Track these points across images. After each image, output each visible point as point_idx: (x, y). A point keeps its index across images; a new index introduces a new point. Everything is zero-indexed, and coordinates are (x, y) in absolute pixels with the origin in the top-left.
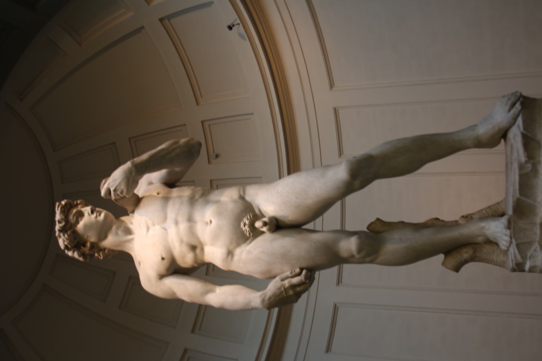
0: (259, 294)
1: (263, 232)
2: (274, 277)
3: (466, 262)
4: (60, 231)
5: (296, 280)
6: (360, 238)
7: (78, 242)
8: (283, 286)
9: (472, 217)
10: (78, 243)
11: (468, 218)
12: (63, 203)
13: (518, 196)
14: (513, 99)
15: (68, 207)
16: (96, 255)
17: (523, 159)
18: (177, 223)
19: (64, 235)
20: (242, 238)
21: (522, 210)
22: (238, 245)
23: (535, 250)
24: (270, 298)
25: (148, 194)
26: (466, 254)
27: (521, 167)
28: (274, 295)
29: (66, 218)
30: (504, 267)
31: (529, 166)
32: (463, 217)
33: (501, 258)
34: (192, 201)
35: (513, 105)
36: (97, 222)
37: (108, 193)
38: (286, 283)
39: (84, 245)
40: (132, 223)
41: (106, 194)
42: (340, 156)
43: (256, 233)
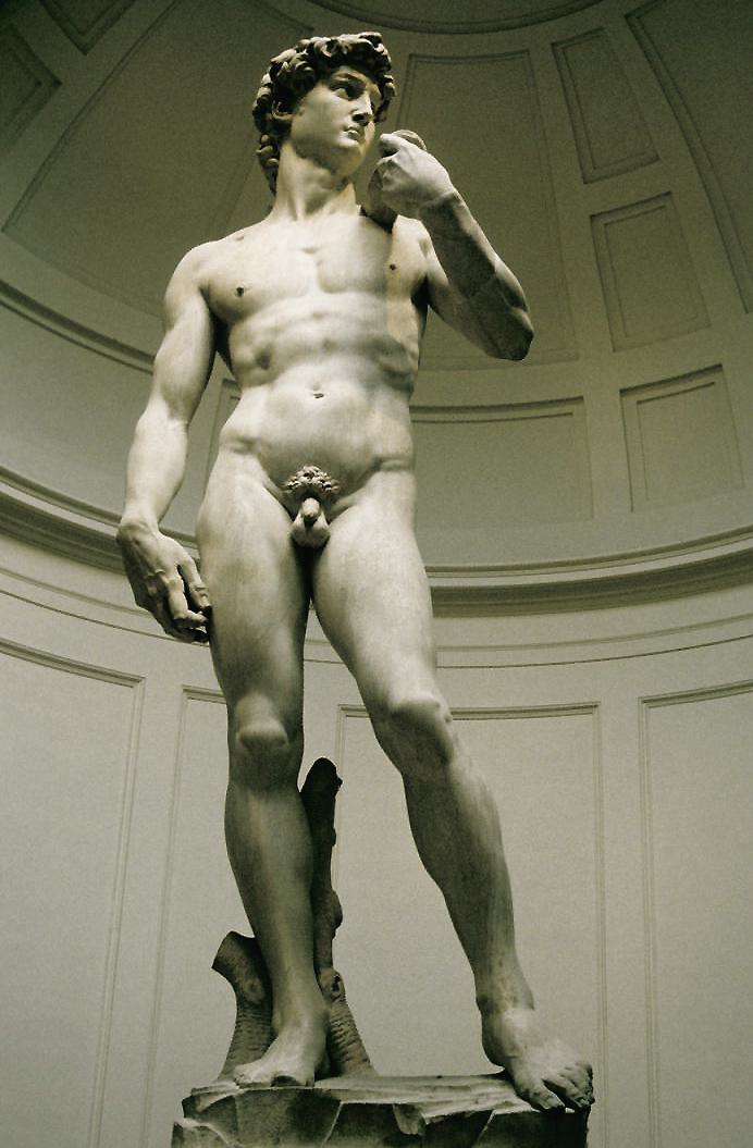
0: (151, 518)
1: (293, 517)
3: (236, 987)
5: (179, 600)
6: (281, 742)
7: (290, 90)
8: (166, 571)
9: (334, 999)
12: (380, 48)
13: (342, 1103)
16: (265, 138)
17: (428, 1115)
18: (318, 316)
19: (303, 58)
20: (279, 469)
24: (138, 543)
25: (396, 245)
27: (409, 1110)
28: (146, 551)
29: (343, 57)
30: (223, 1072)
31: (415, 1129)
32: (338, 979)
34: (375, 349)
36: (335, 132)
37: (389, 149)
38: (174, 578)
39: (283, 110)
40: (333, 212)
41: (383, 144)
43: (291, 502)
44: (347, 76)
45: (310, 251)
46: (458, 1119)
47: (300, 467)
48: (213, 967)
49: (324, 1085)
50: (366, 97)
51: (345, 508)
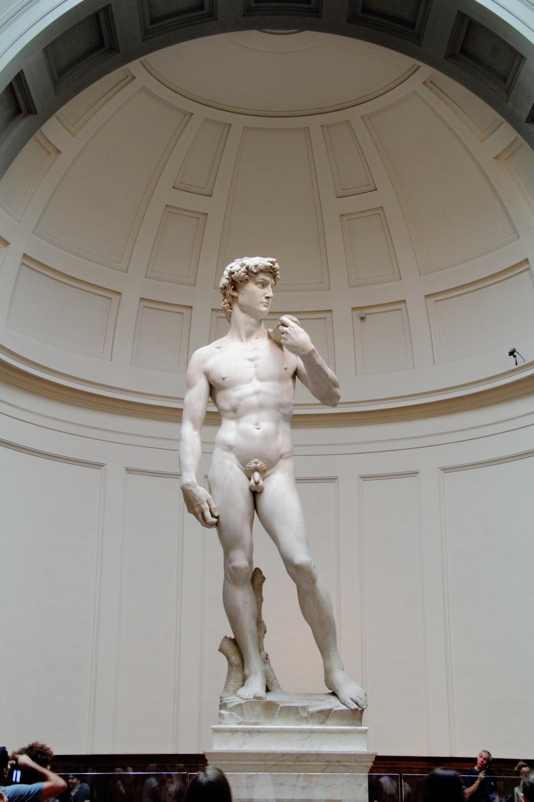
0: (195, 481)
1: (250, 479)
2: (210, 492)
3: (228, 658)
4: (247, 268)
5: (208, 514)
6: (246, 568)
8: (203, 503)
10: (237, 283)
11: (266, 659)
12: (277, 266)
14: (360, 702)
15: (272, 271)
16: (226, 300)
17: (311, 710)
18: (257, 393)
21: (270, 709)
22: (238, 457)
23: (237, 718)
24: (191, 491)
26: (235, 659)
27: (304, 708)
28: (194, 495)
30: (224, 690)
32: (267, 655)
33: (231, 689)
34: (279, 406)
38: (205, 506)
39: (235, 289)
40: (257, 338)
42: (361, 478)
44: (263, 279)
45: (251, 360)
46: (321, 712)
47: (252, 460)
48: (219, 650)
49: (270, 697)
50: (270, 287)
51: (269, 475)
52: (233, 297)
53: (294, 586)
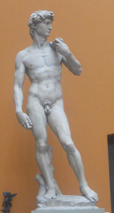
0: (22, 111)
1: (45, 108)
2: (28, 115)
5: (28, 125)
6: (46, 146)
12: (53, 15)
14: (96, 199)
16: (31, 30)
17: (75, 202)
18: (46, 71)
19: (39, 18)
22: (40, 99)
24: (20, 115)
27: (72, 202)
34: (56, 77)
35: (94, 199)
38: (27, 121)
39: (35, 26)
40: (45, 47)
43: (44, 106)
44: (47, 21)
45: (44, 57)
52: (34, 29)
53: (66, 153)
